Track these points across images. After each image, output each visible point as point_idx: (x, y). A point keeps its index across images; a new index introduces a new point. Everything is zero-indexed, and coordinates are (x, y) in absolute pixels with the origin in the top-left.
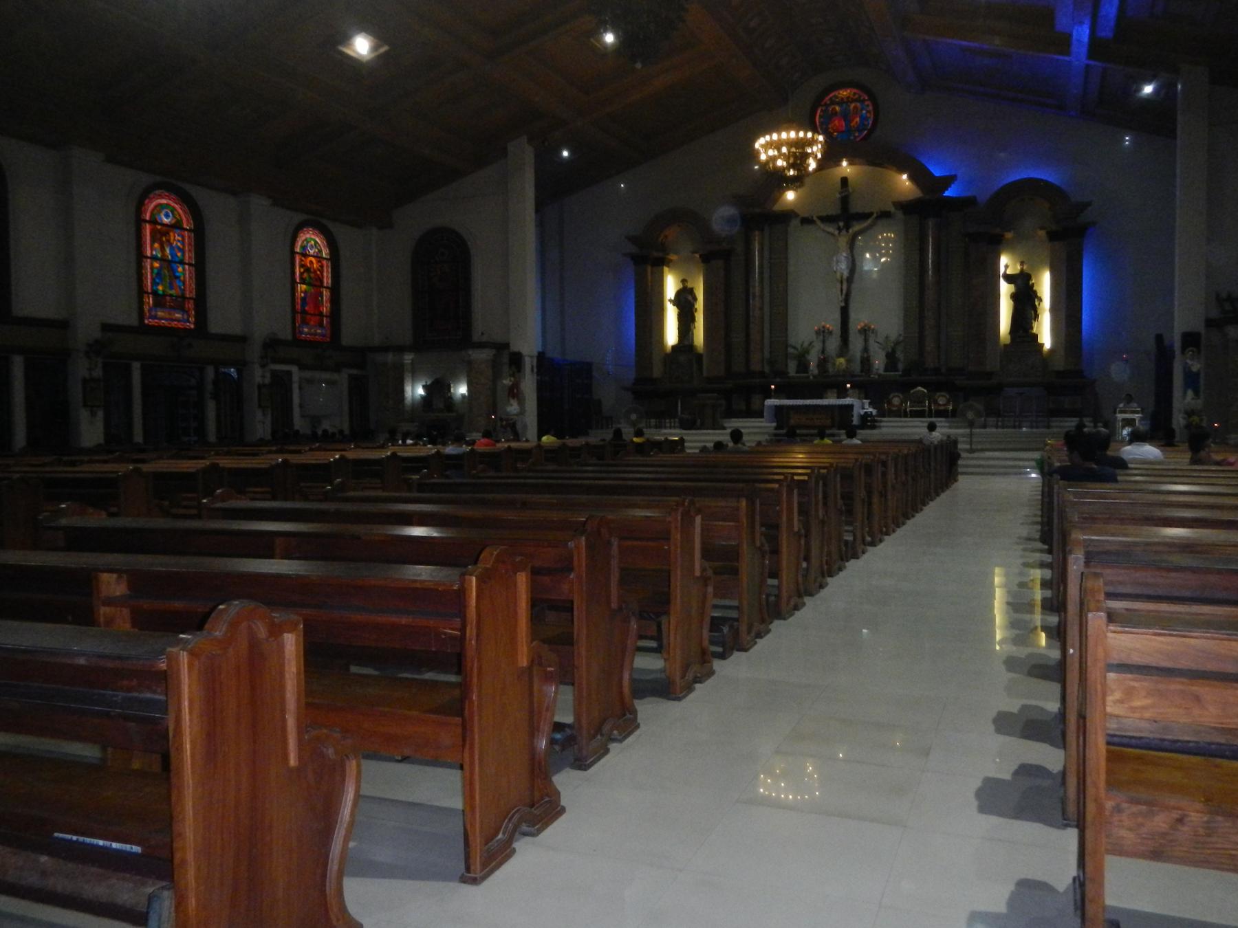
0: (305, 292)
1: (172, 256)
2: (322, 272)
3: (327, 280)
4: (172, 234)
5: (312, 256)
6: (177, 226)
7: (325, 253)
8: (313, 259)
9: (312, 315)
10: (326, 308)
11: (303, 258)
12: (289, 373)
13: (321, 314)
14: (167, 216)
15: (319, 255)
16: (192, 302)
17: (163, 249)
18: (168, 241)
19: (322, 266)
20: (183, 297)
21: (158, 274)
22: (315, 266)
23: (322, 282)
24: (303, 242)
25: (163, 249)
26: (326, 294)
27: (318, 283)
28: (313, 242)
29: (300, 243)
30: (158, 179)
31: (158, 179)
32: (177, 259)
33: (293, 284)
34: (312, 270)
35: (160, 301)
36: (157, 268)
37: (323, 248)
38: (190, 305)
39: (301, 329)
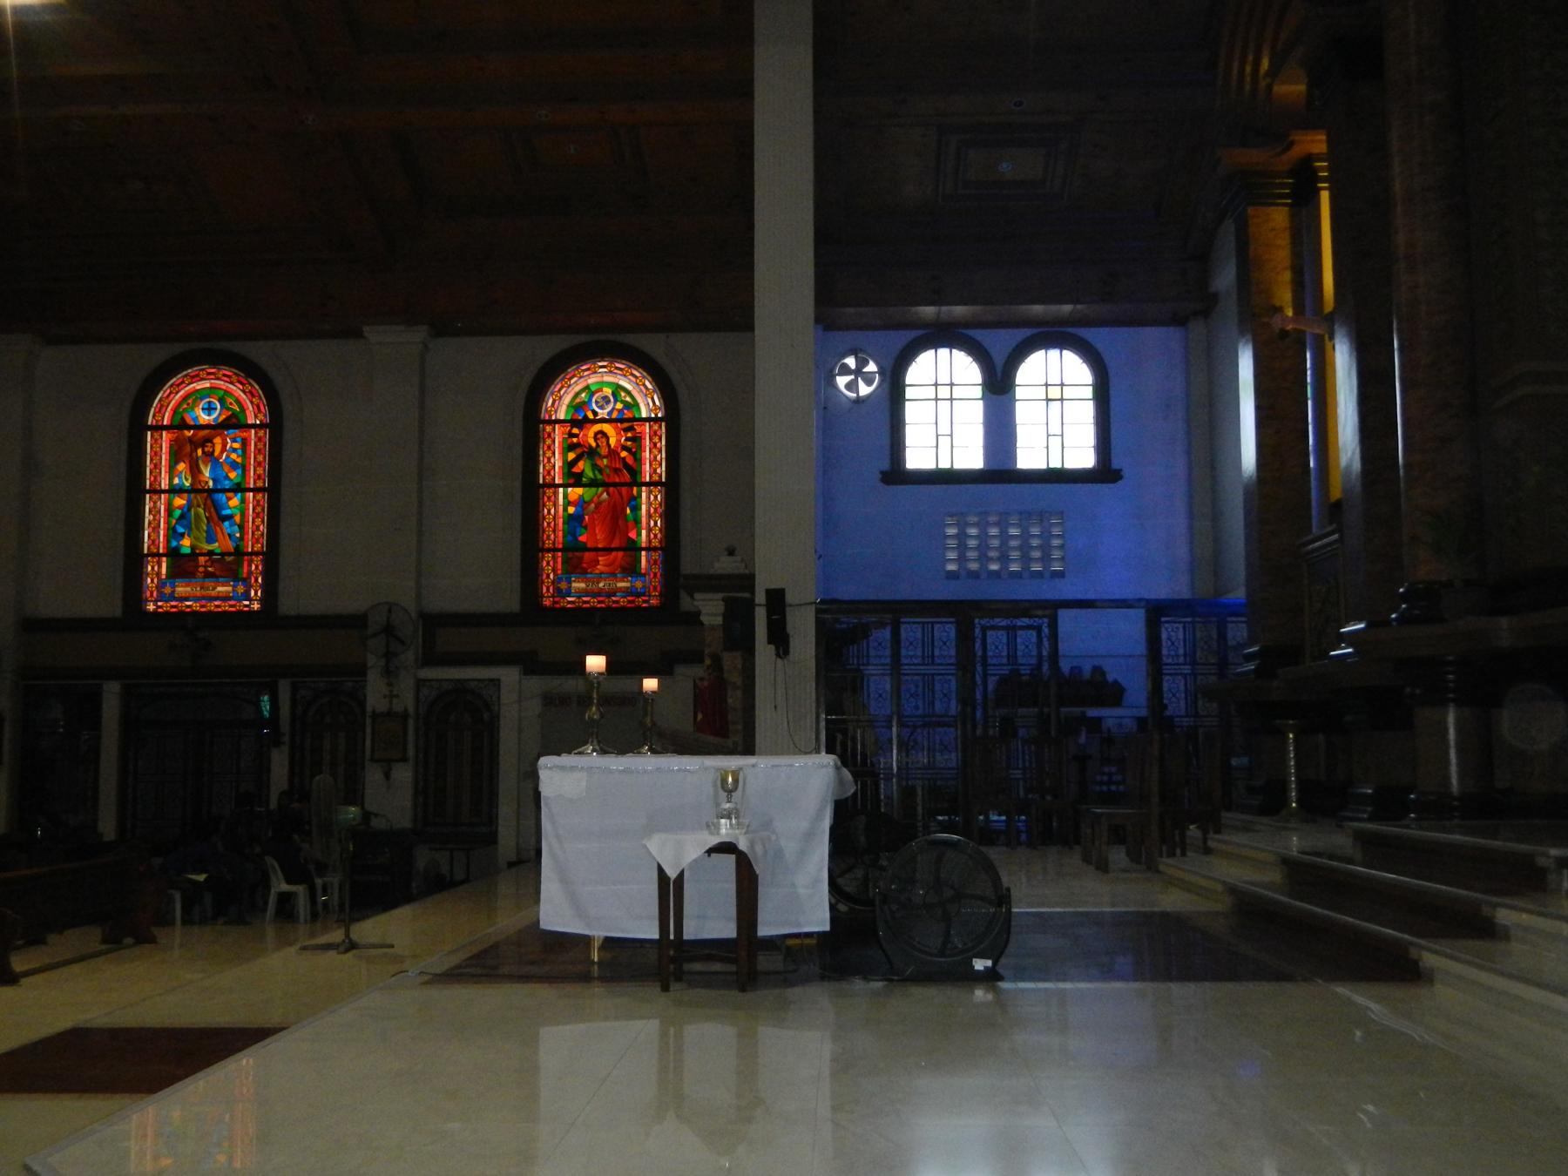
0: (580, 503)
1: (215, 481)
2: (636, 453)
3: (653, 463)
4: (218, 440)
5: (603, 421)
6: (232, 422)
7: (648, 404)
8: (607, 428)
9: (596, 550)
10: (649, 530)
11: (575, 431)
12: (496, 683)
13: (633, 548)
14: (209, 409)
15: (627, 414)
16: (257, 560)
17: (195, 471)
18: (209, 455)
19: (637, 439)
20: (239, 553)
21: (182, 517)
22: (613, 441)
23: (634, 472)
24: (577, 394)
25: (195, 471)
26: (649, 501)
27: (627, 477)
28: (608, 391)
29: (567, 400)
30: (177, 348)
31: (177, 348)
32: (227, 485)
33: (532, 492)
34: (604, 451)
35: (183, 566)
36: (180, 507)
37: (639, 399)
38: (256, 565)
39: (563, 585)
